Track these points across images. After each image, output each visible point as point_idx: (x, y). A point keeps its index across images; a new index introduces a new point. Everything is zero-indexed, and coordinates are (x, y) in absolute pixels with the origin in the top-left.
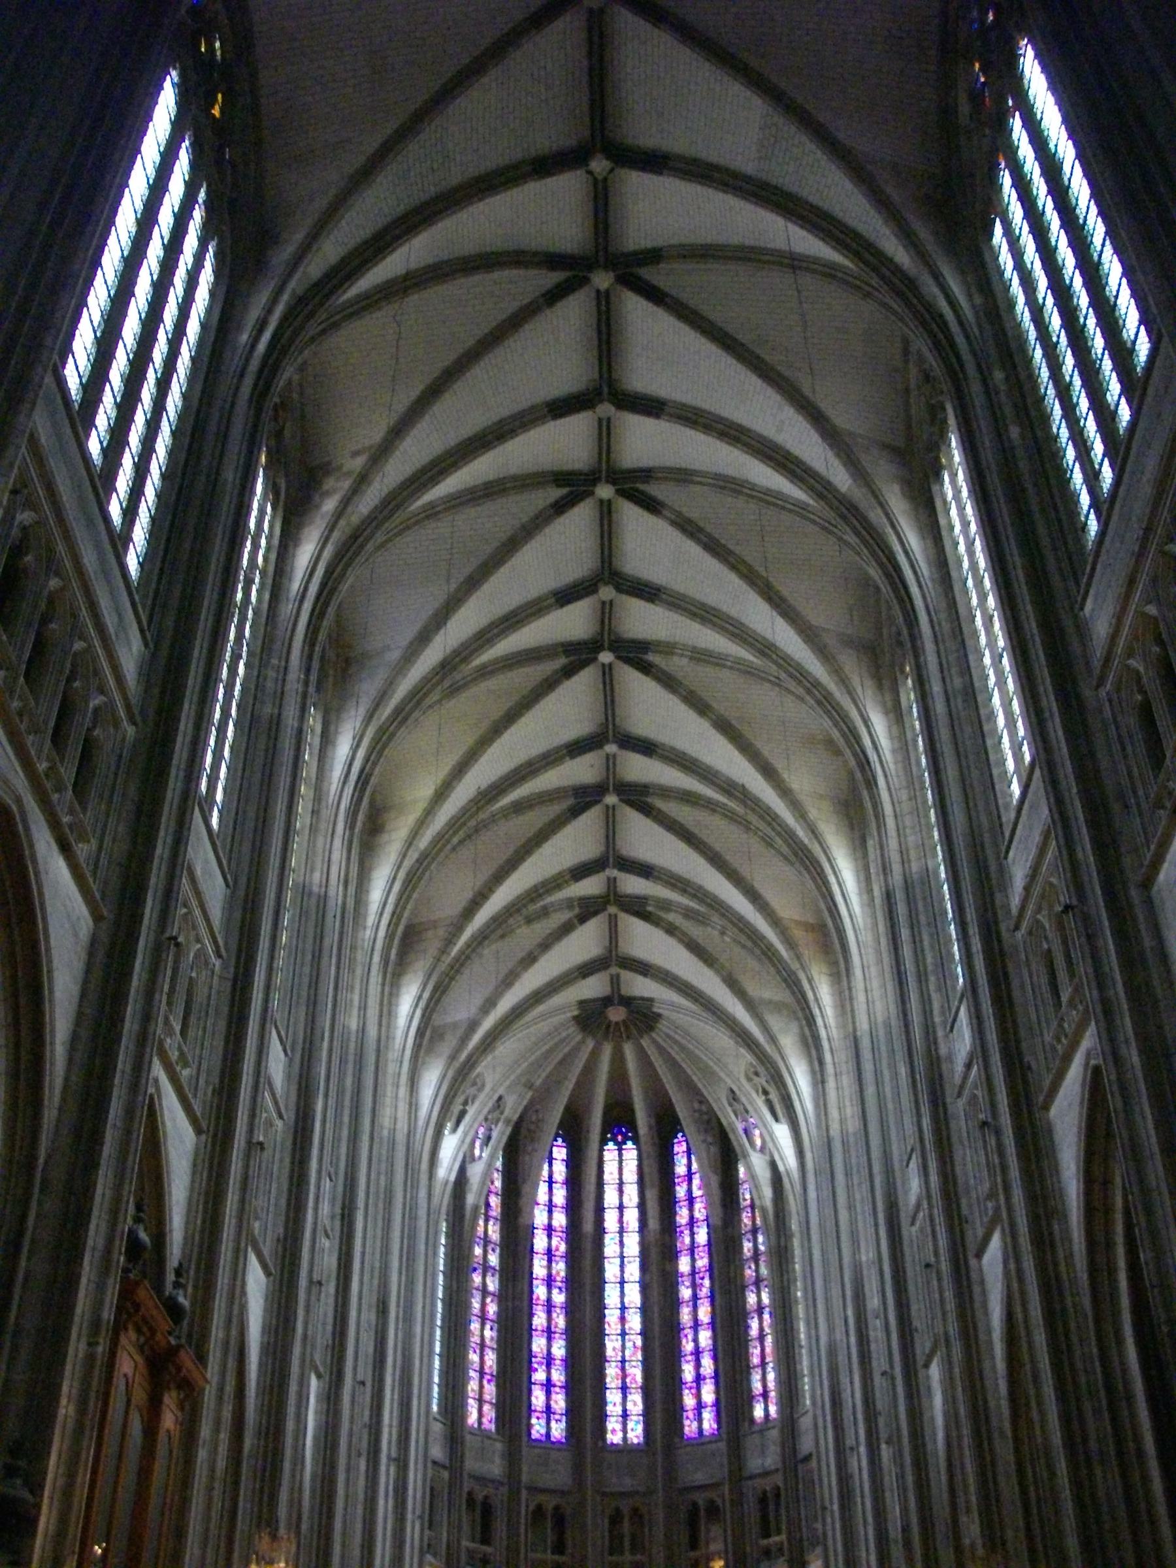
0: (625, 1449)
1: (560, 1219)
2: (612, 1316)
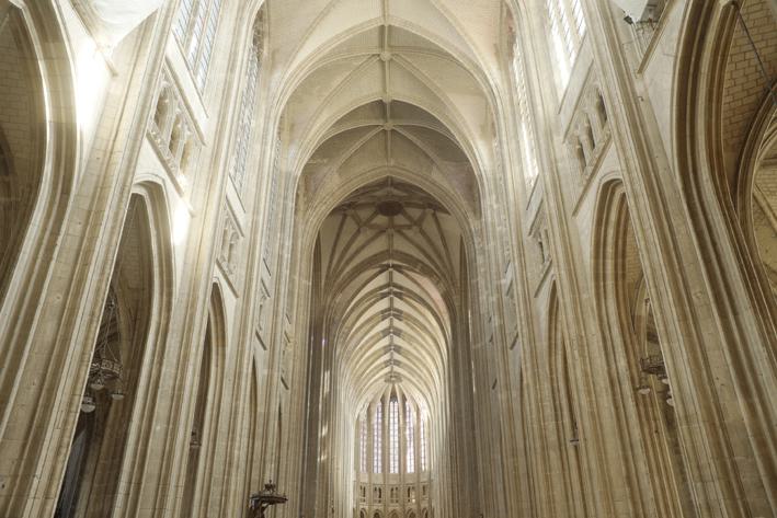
0: (394, 475)
1: (380, 421)
2: (392, 444)
